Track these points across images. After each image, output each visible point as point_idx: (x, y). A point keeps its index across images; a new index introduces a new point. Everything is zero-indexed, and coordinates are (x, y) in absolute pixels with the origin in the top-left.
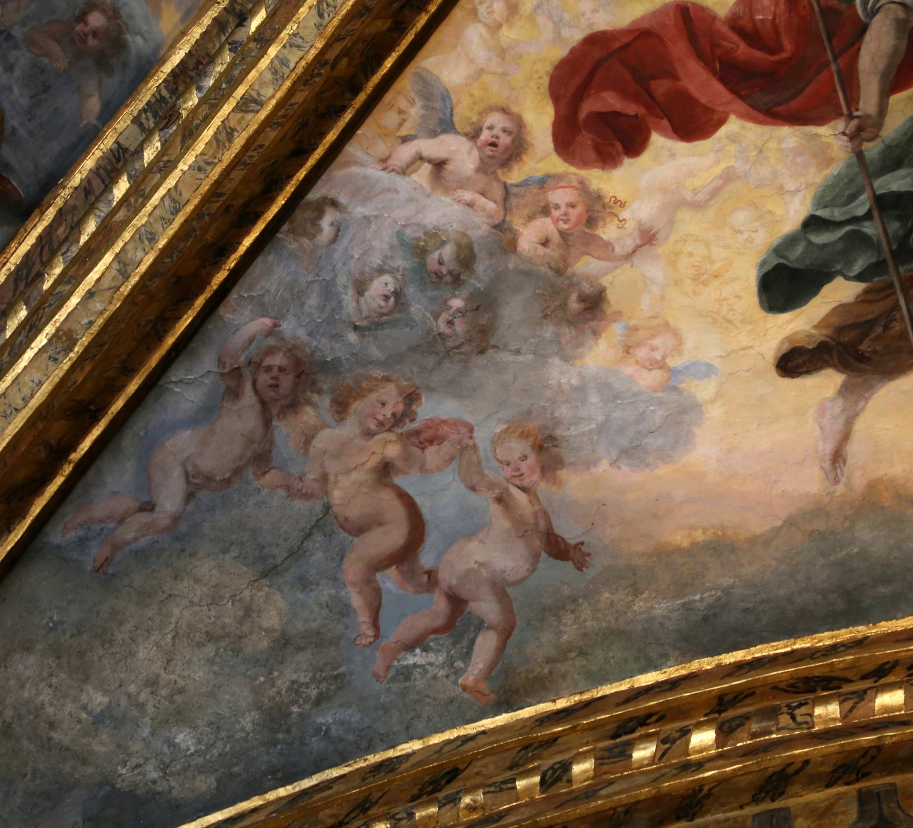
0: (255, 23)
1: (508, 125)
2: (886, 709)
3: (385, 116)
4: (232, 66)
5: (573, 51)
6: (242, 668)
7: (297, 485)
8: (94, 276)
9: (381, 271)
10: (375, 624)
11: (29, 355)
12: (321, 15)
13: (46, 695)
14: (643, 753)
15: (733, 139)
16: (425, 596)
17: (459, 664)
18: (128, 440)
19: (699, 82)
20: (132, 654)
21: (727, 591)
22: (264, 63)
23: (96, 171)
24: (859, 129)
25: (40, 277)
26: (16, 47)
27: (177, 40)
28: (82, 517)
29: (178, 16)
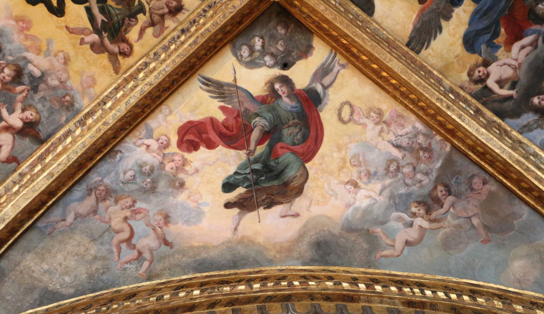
1: (166, 139)
2: (240, 290)
3: (136, 133)
4: (102, 114)
6: (84, 263)
7: (103, 219)
8: (60, 160)
9: (130, 170)
10: (119, 256)
11: (41, 177)
13: (32, 264)
14: (182, 294)
15: (220, 151)
16: (132, 251)
17: (139, 268)
18: (61, 203)
19: (213, 136)
20: (56, 256)
21: (206, 258)
22: (111, 114)
23: (63, 135)
24: (249, 153)
25: (45, 158)
28: (47, 220)
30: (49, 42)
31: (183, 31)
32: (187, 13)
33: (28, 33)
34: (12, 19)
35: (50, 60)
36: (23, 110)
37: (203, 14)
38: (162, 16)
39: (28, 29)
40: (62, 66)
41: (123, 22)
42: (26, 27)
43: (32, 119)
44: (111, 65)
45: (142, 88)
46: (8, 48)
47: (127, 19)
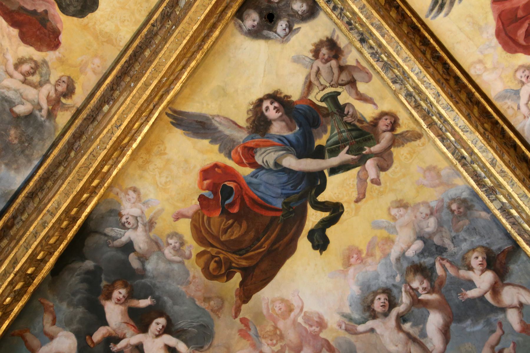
0: (466, 154)
1: (521, 71)
3: (509, 114)
4: (478, 165)
5: (500, 43)
12: (467, 131)
22: (480, 154)
23: (507, 219)
26: (458, 236)
27: (467, 181)
29: (458, 178)
30: (376, 226)
31: (363, 40)
32: (338, 32)
33: (365, 252)
34: (347, 271)
35: (401, 227)
36: (470, 268)
37: (339, 11)
38: (342, 69)
39: (359, 252)
40: (409, 211)
41: (349, 124)
42: (357, 254)
43: (483, 258)
44: (409, 144)
45: (443, 108)
46: (385, 280)
47: (345, 118)
